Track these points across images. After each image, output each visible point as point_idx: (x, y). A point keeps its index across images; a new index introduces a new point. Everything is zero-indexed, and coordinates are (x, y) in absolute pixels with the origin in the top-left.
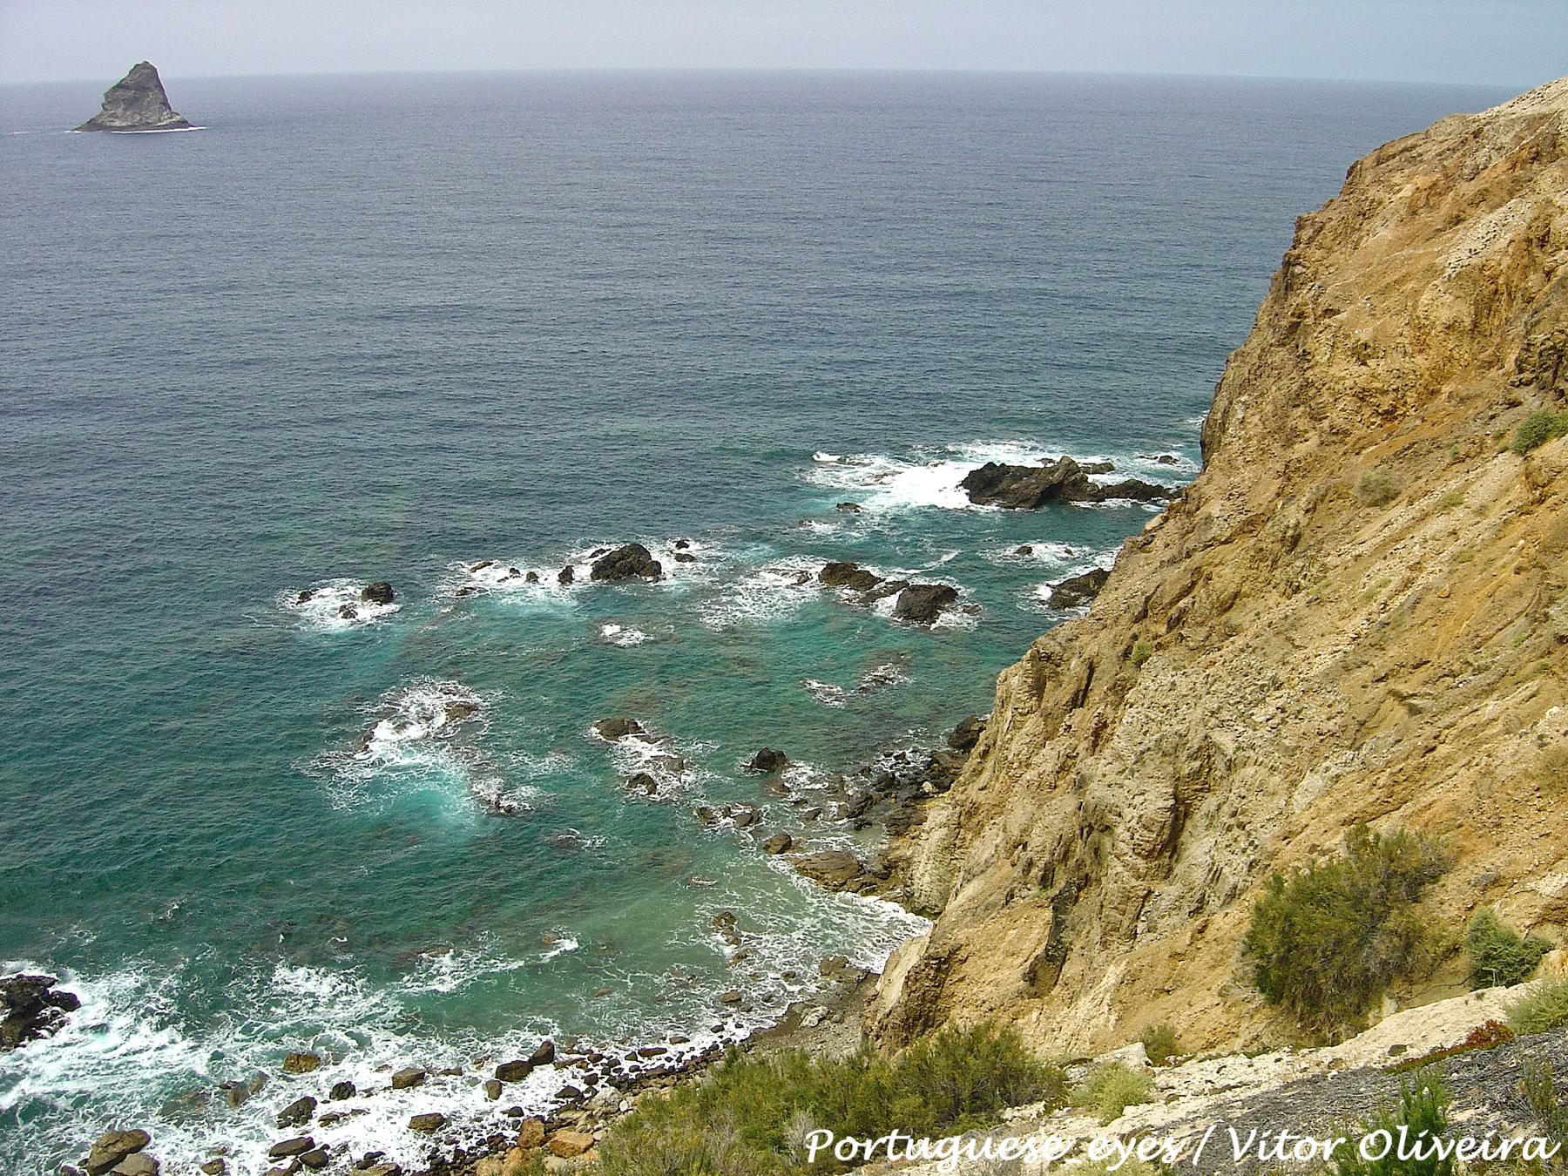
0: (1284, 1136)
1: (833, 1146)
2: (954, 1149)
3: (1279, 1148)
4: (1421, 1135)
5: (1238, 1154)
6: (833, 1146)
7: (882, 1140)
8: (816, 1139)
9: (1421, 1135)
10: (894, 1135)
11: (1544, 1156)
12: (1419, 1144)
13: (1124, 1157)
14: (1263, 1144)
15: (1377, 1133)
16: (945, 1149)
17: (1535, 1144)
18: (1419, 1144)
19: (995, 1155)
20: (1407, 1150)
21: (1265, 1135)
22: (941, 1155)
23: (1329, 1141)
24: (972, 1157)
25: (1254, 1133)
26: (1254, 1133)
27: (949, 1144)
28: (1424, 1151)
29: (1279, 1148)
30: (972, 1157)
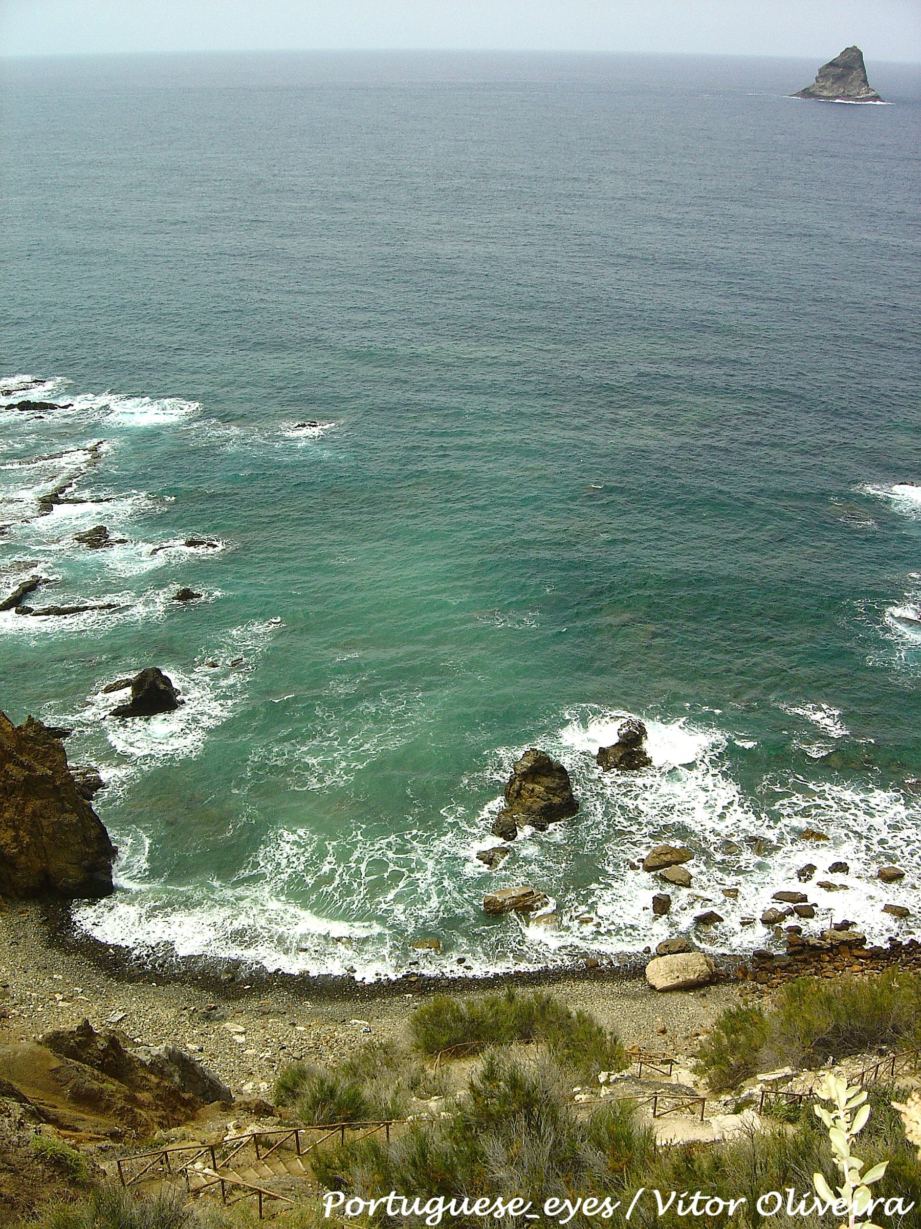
0: (697, 1197)
1: (344, 1204)
2: (440, 1206)
3: (693, 1206)
4: (805, 1196)
5: (661, 1211)
6: (344, 1204)
7: (383, 1200)
8: (331, 1198)
9: (805, 1196)
10: (392, 1196)
11: (901, 1212)
12: (803, 1203)
13: (572, 1212)
14: (681, 1203)
15: (771, 1193)
16: (432, 1207)
17: (894, 1204)
18: (803, 1203)
19: (471, 1211)
20: (794, 1207)
21: (682, 1196)
22: (429, 1212)
23: (373, 1201)
24: (453, 1213)
25: (674, 1194)
26: (674, 1194)
27: (435, 1203)
28: (808, 1207)
29: (693, 1206)
30: (453, 1213)
